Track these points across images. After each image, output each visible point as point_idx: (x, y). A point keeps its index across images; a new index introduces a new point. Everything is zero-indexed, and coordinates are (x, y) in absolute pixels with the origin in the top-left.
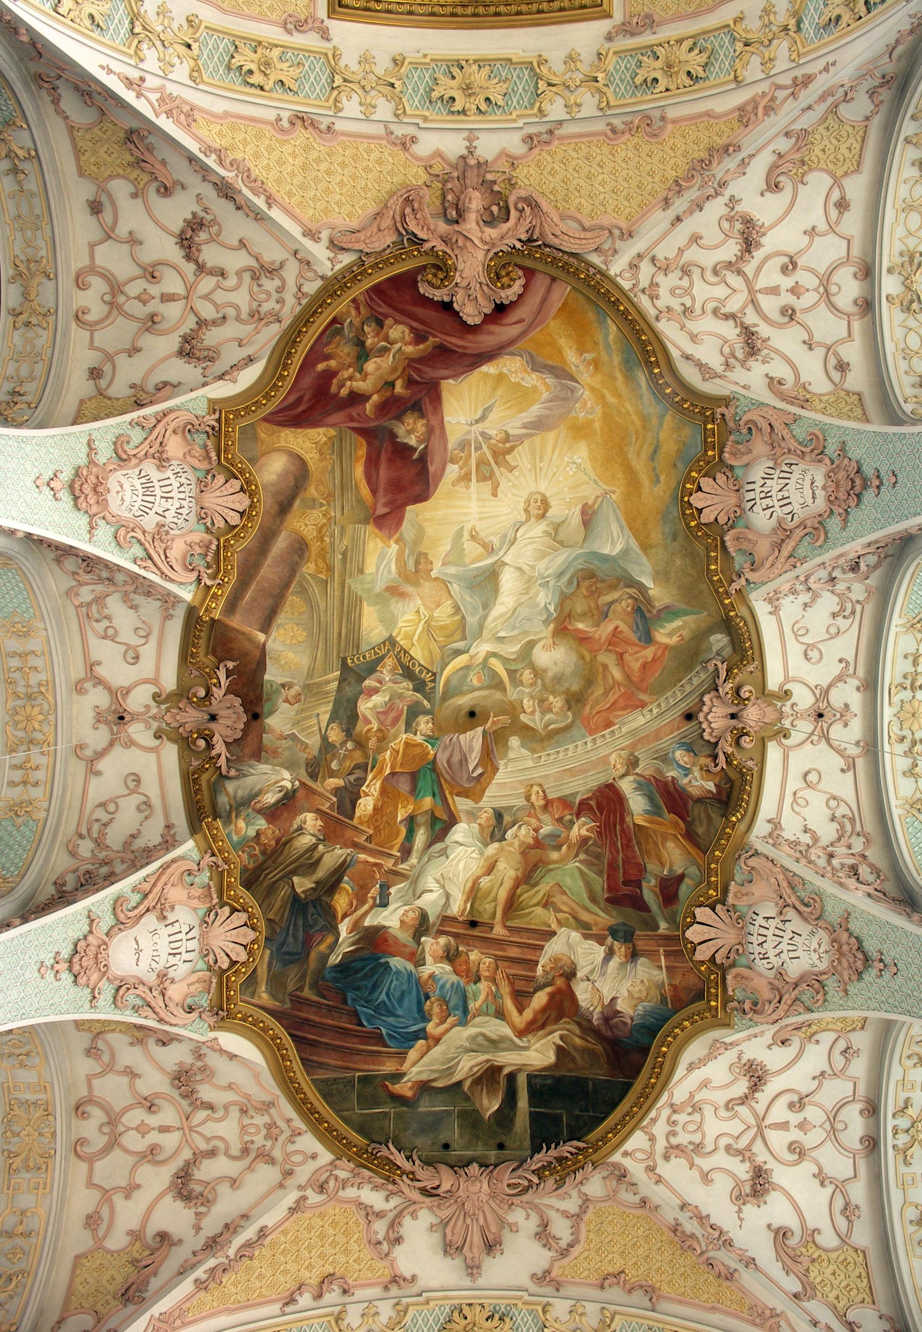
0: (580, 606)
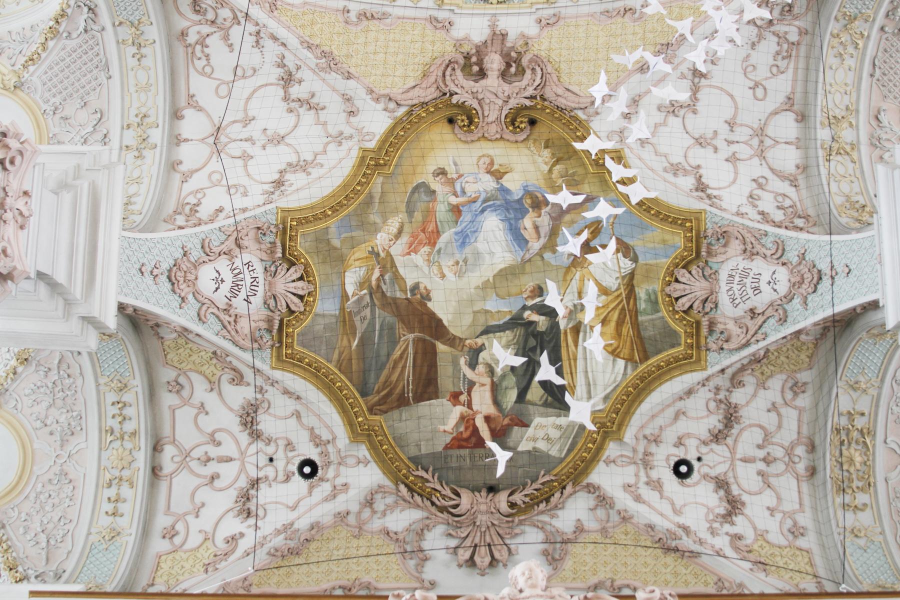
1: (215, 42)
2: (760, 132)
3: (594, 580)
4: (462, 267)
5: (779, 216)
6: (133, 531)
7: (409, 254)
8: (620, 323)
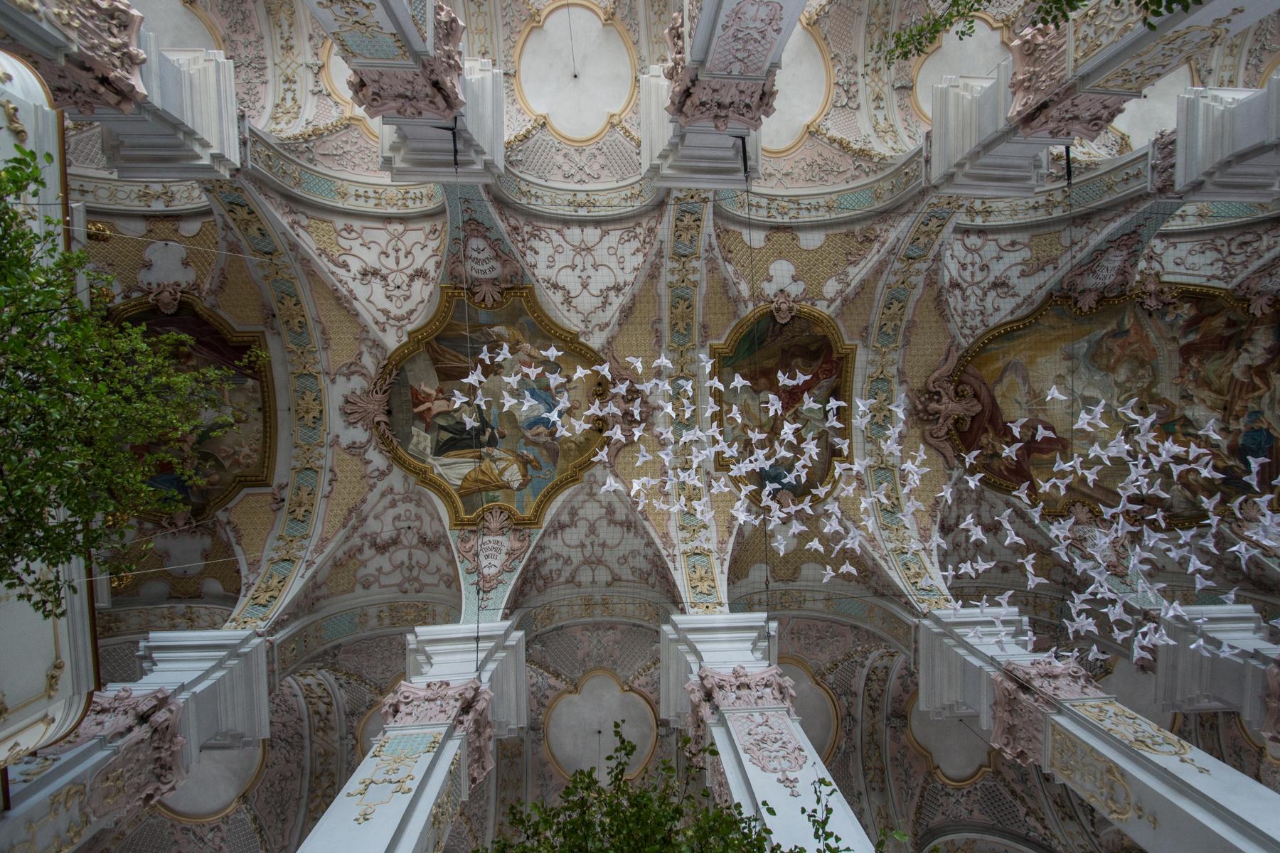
0: (1105, 361)
1: (635, 244)
2: (600, 562)
3: (337, 470)
5: (545, 571)
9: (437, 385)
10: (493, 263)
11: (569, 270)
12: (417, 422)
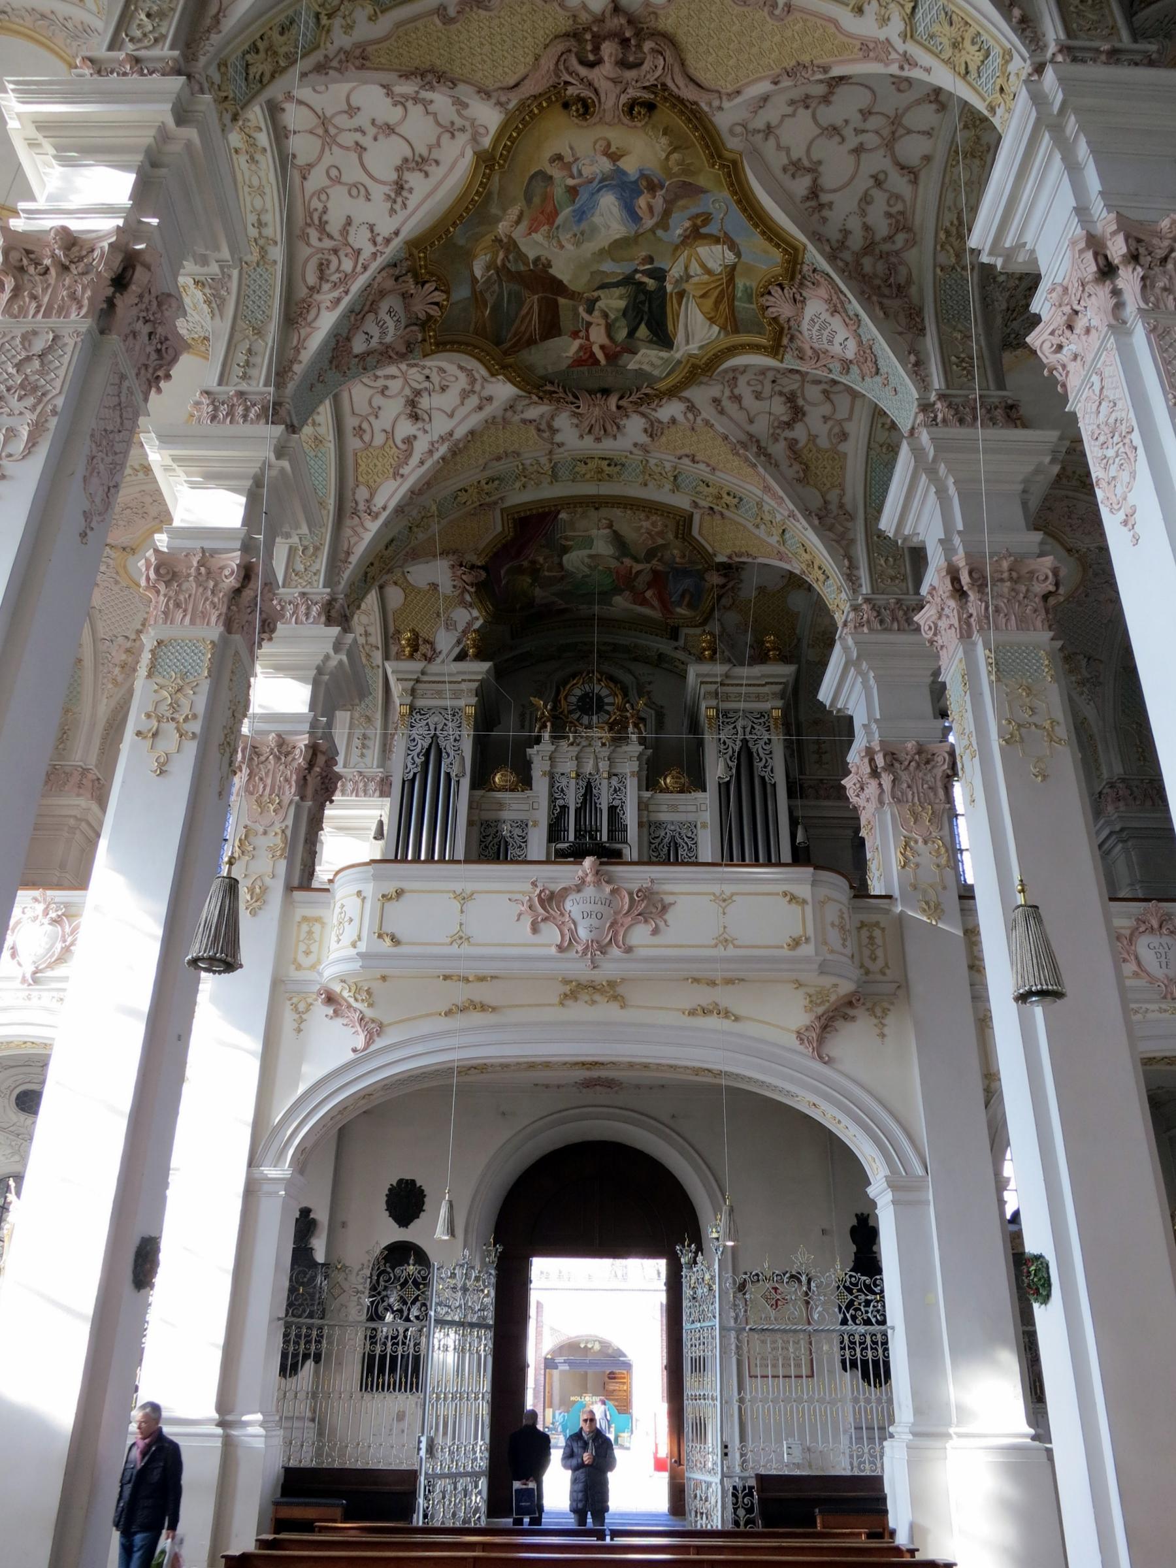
2: (896, 121)
3: (680, 452)
4: (578, 243)
5: (882, 228)
6: (331, 438)
7: (530, 234)
8: (717, 303)
9: (565, 338)
10: (383, 315)
11: (367, 157)
12: (620, 362)
